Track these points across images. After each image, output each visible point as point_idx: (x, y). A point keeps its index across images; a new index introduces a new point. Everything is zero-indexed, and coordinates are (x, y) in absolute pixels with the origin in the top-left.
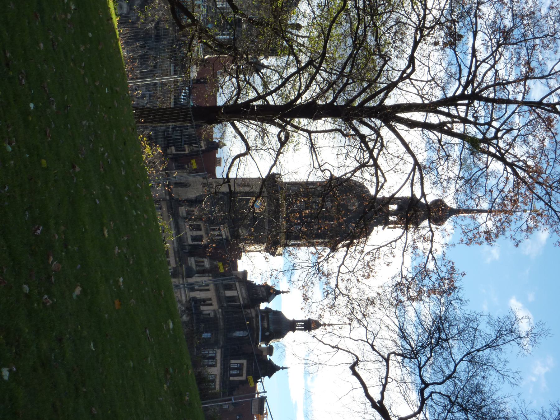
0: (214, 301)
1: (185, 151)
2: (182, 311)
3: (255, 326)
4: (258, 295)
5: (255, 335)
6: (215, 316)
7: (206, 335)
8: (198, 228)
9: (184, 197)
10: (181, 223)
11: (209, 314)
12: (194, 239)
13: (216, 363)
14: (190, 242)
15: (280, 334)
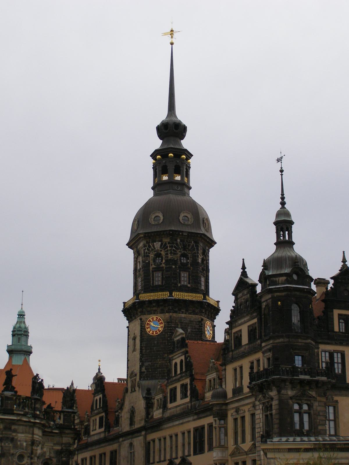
0: (254, 357)
1: (103, 416)
2: (264, 397)
3: (283, 294)
4: (247, 301)
5: (298, 293)
6: (270, 350)
7: (298, 361)
8: (173, 391)
9: (143, 413)
10: (168, 414)
11: (269, 359)
12: (184, 396)
13: (337, 352)
14: (188, 400)
15: (299, 267)
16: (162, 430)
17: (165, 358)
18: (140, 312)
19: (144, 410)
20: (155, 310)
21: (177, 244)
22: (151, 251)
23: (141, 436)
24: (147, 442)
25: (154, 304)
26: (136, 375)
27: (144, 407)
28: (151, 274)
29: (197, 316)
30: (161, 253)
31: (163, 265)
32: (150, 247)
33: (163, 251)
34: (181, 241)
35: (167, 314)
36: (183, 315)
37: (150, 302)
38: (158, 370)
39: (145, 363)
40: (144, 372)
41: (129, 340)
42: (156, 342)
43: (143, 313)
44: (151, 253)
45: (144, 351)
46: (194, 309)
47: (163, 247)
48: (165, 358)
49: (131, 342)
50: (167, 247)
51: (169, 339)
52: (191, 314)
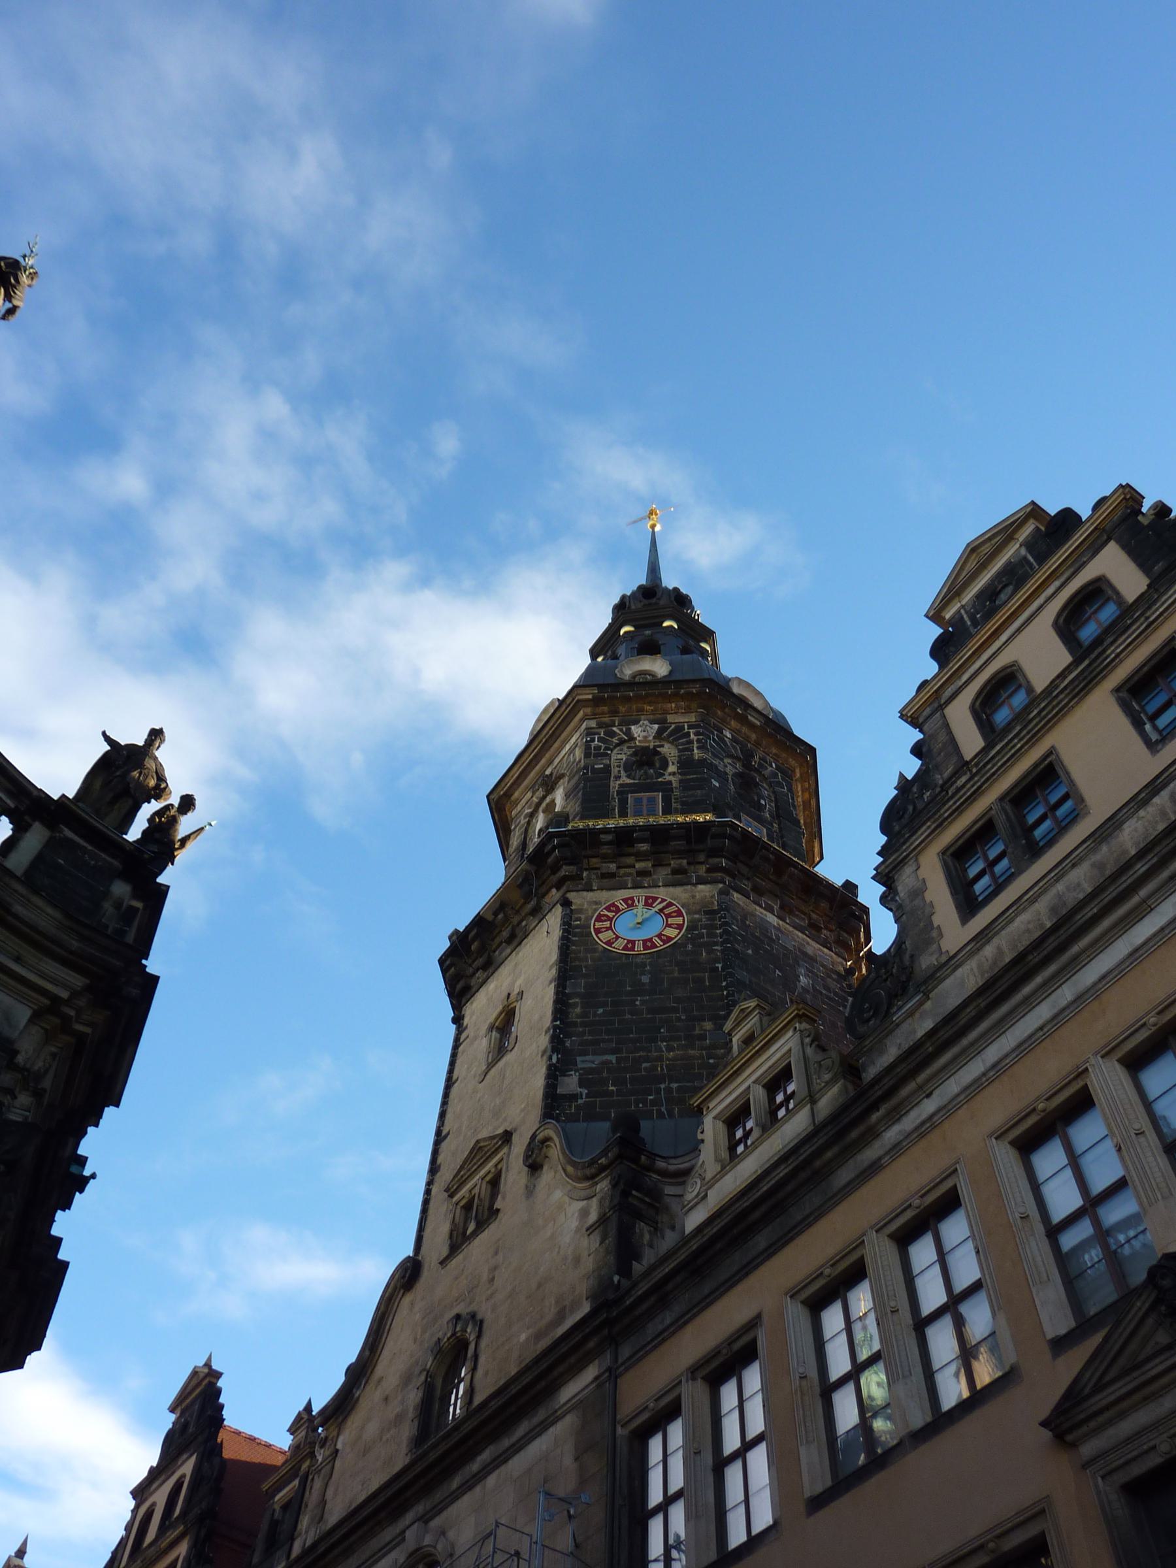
16: (874, 1168)
17: (702, 1037)
18: (558, 889)
19: (596, 1238)
20: (643, 873)
21: (722, 739)
22: (617, 745)
23: (543, 1427)
24: (620, 1431)
25: (644, 847)
26: (507, 1137)
27: (593, 1217)
28: (613, 798)
29: (825, 950)
30: (659, 753)
31: (671, 778)
32: (613, 734)
33: (667, 745)
34: (734, 739)
35: (700, 887)
36: (772, 919)
37: (624, 837)
38: (663, 1086)
39: (579, 1059)
40: (574, 1097)
41: (458, 1062)
42: (645, 979)
43: (575, 881)
44: (615, 751)
45: (578, 1010)
46: (814, 916)
47: (670, 735)
48: (702, 1037)
49: (479, 1046)
50: (688, 734)
51: (720, 966)
52: (803, 933)
